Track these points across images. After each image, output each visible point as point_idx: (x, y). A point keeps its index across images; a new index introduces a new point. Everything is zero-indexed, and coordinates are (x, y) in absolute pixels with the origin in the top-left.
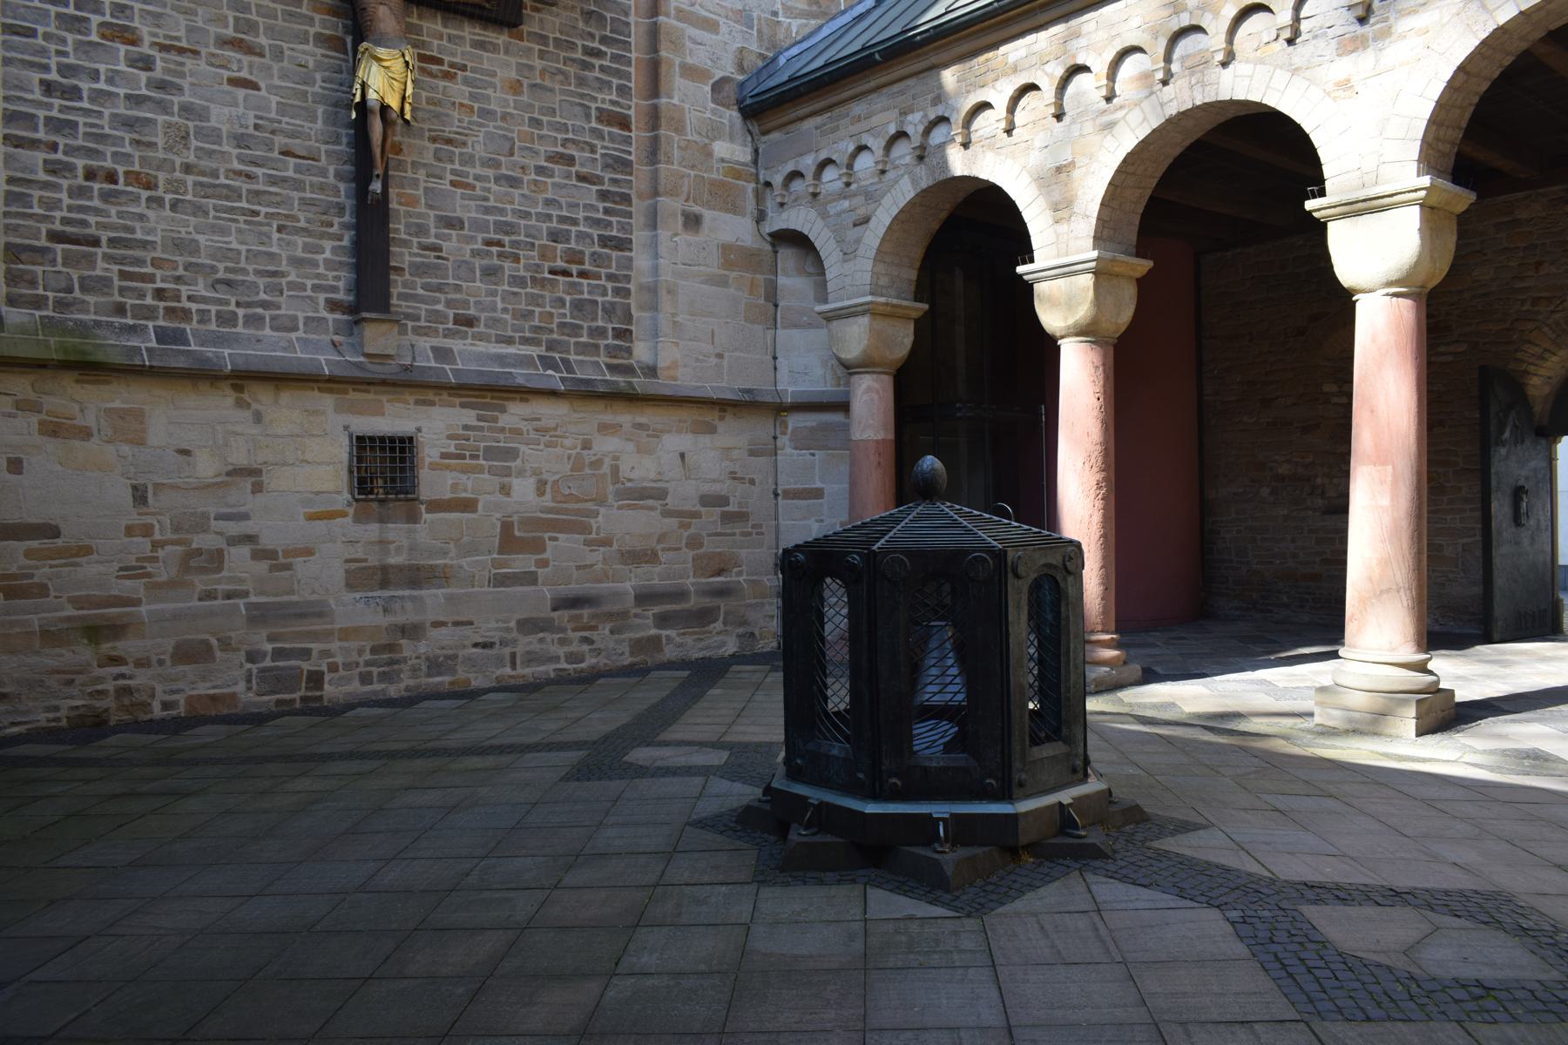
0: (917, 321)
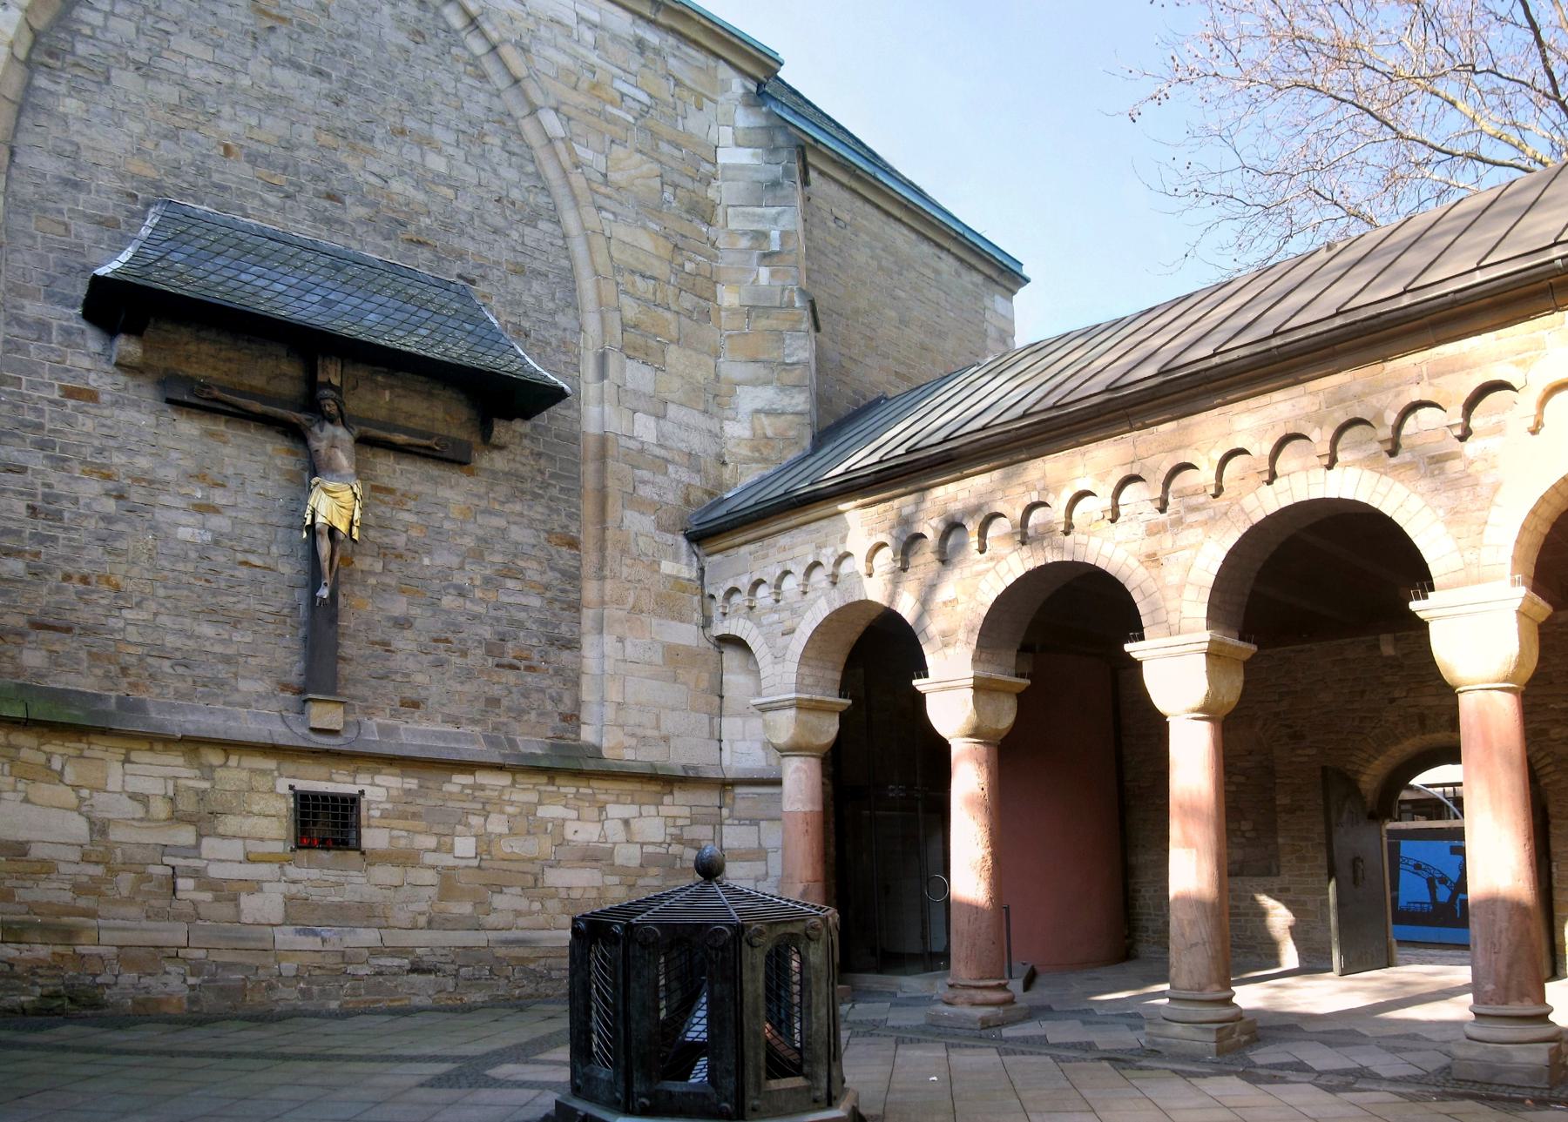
0: (841, 715)
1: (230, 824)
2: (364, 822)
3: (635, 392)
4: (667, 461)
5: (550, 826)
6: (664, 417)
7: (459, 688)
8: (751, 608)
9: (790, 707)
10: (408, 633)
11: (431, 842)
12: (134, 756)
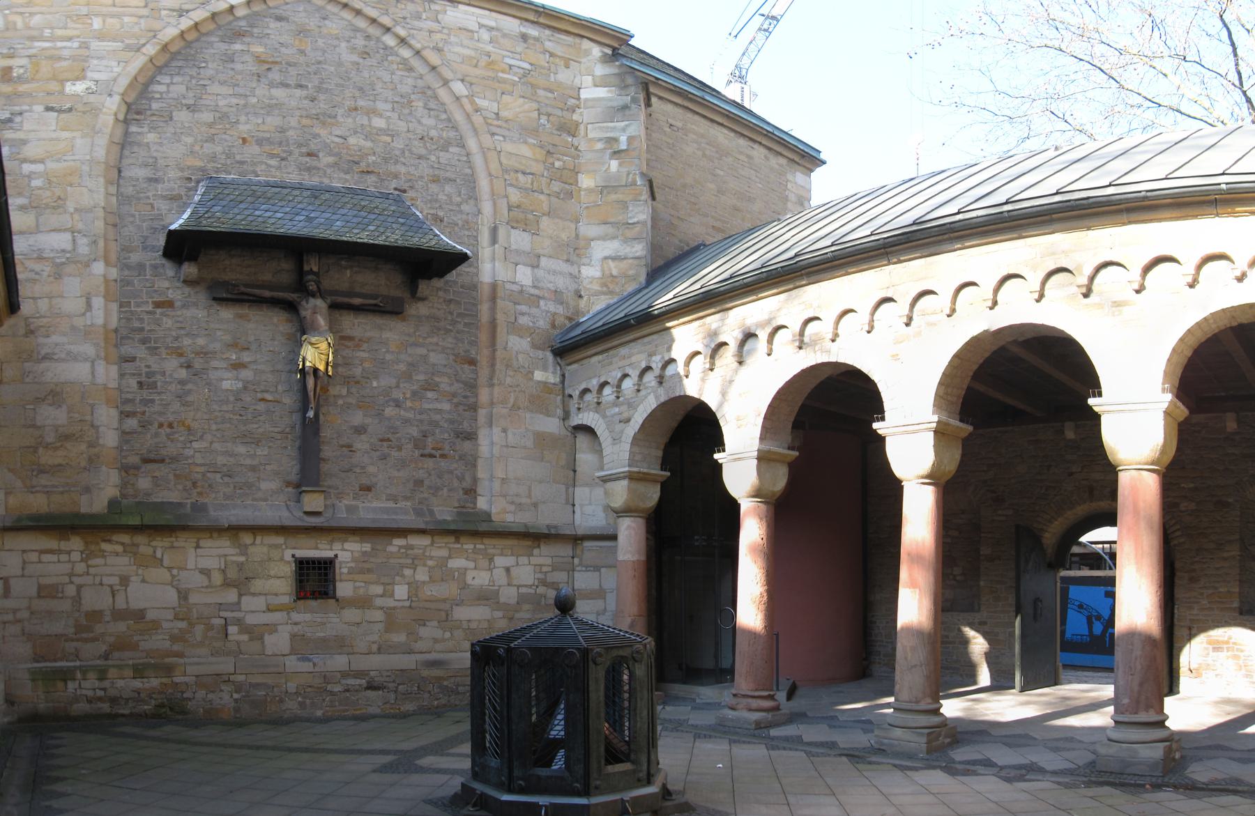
1: (257, 585)
2: (337, 577)
3: (517, 251)
4: (539, 297)
5: (456, 574)
6: (538, 266)
7: (396, 474)
8: (599, 403)
9: (624, 478)
10: (363, 437)
11: (378, 589)
12: (202, 543)
